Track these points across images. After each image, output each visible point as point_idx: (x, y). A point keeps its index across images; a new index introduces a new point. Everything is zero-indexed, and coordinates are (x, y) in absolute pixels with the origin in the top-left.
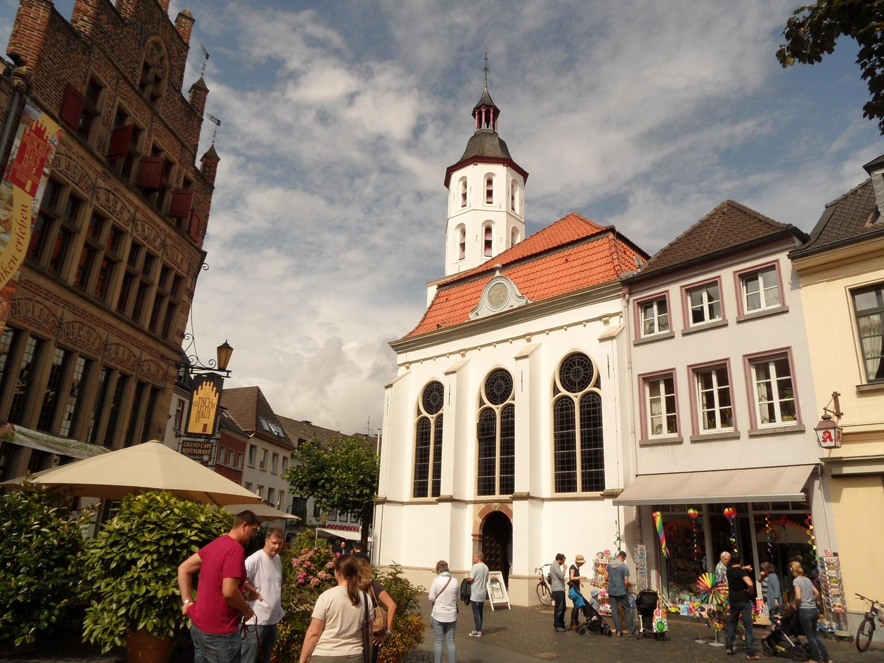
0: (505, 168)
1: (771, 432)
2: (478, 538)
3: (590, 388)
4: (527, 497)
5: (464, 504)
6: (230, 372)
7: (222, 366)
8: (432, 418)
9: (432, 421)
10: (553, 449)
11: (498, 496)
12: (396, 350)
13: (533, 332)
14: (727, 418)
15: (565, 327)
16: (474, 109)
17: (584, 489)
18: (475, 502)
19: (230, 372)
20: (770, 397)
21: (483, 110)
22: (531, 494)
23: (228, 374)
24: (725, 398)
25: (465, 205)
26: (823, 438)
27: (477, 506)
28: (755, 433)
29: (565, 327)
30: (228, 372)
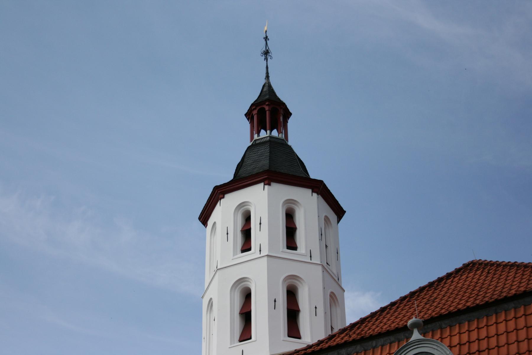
16: (252, 105)
21: (267, 108)
25: (250, 249)
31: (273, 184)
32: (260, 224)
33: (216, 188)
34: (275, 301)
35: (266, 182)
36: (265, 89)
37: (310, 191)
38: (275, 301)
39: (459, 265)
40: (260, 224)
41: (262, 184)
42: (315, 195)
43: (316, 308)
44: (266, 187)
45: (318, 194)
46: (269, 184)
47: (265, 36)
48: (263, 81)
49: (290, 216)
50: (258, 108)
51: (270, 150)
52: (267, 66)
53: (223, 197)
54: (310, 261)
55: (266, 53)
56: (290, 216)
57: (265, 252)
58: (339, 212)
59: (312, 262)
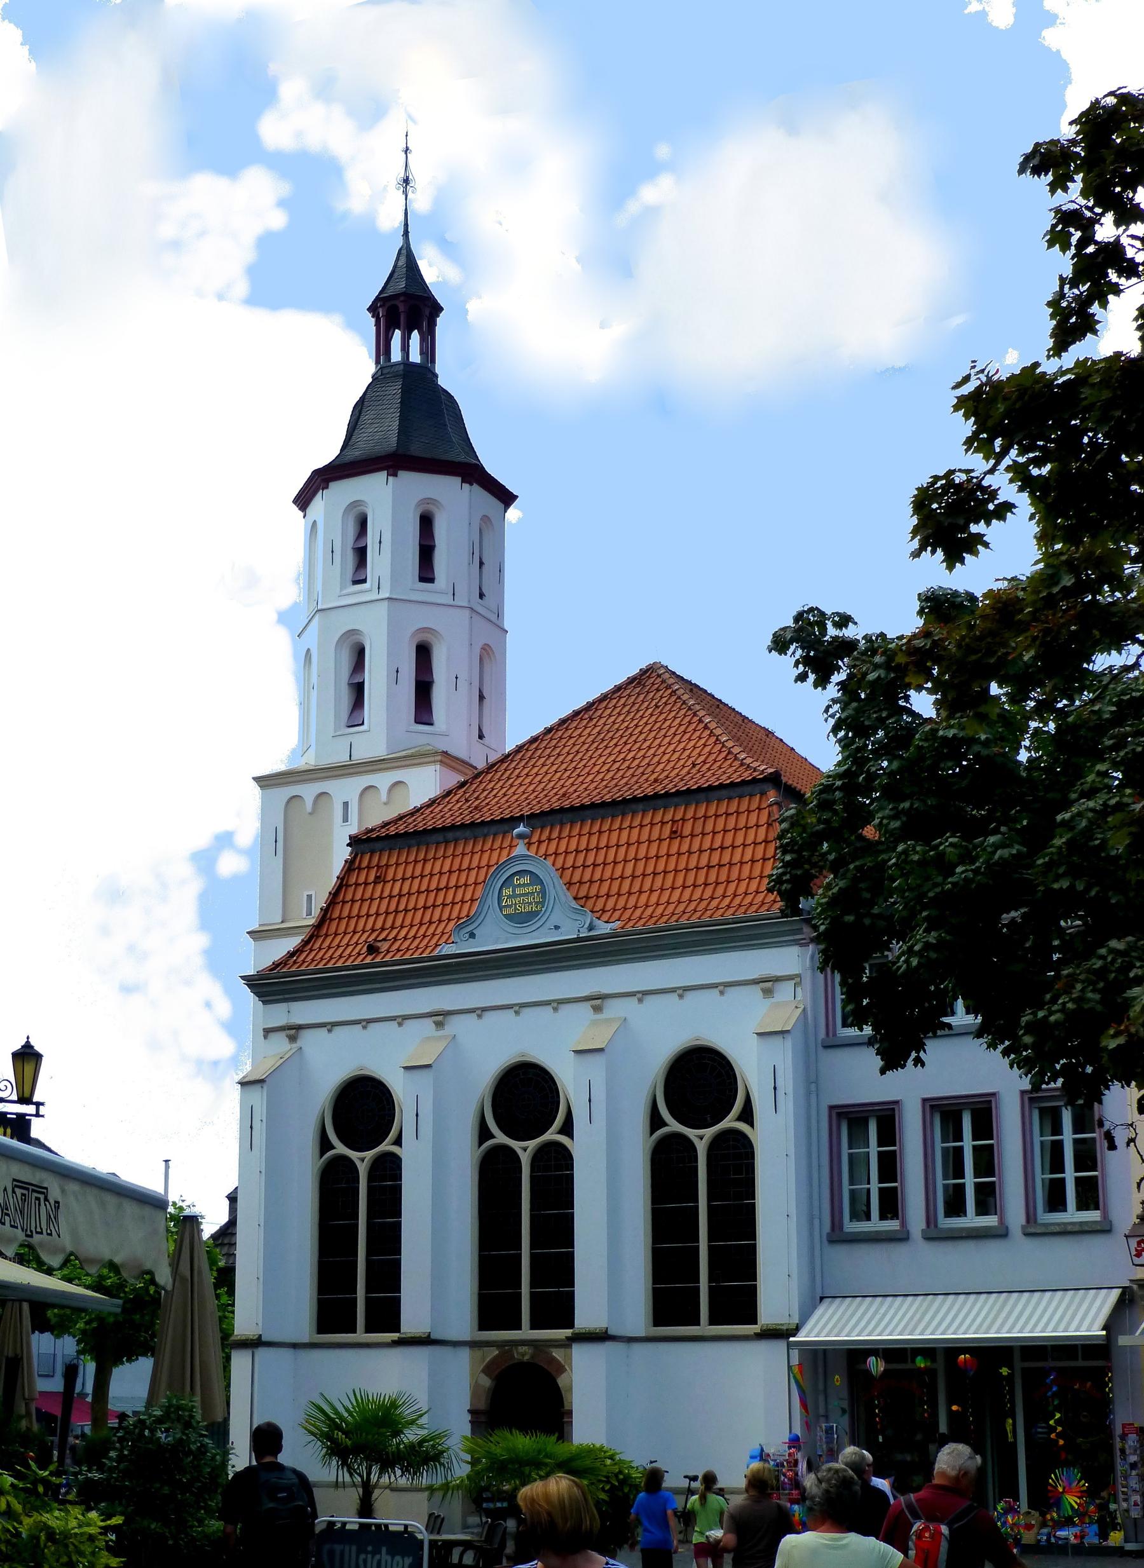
1: (1058, 1229)
2: (483, 1419)
3: (729, 1122)
6: (42, 1104)
7: (27, 1095)
8: (363, 1160)
11: (526, 1332)
12: (259, 995)
13: (606, 992)
14: (987, 1199)
15: (680, 992)
18: (473, 1345)
19: (42, 1104)
20: (1057, 1164)
21: (402, 308)
23: (38, 1110)
24: (986, 1161)
25: (364, 581)
26: (1136, 1250)
27: (478, 1353)
28: (1032, 1230)
29: (680, 992)
30: (38, 1104)
31: (401, 473)
32: (380, 542)
33: (317, 473)
34: (397, 671)
35: (391, 471)
36: (400, 263)
37: (459, 479)
38: (397, 671)
39: (634, 671)
40: (380, 542)
42: (466, 486)
43: (457, 678)
44: (391, 478)
45: (471, 484)
46: (395, 475)
48: (400, 242)
49: (426, 522)
50: (388, 304)
51: (401, 398)
52: (406, 209)
54: (451, 602)
55: (406, 181)
56: (426, 522)
57: (385, 594)
58: (506, 498)
59: (455, 603)
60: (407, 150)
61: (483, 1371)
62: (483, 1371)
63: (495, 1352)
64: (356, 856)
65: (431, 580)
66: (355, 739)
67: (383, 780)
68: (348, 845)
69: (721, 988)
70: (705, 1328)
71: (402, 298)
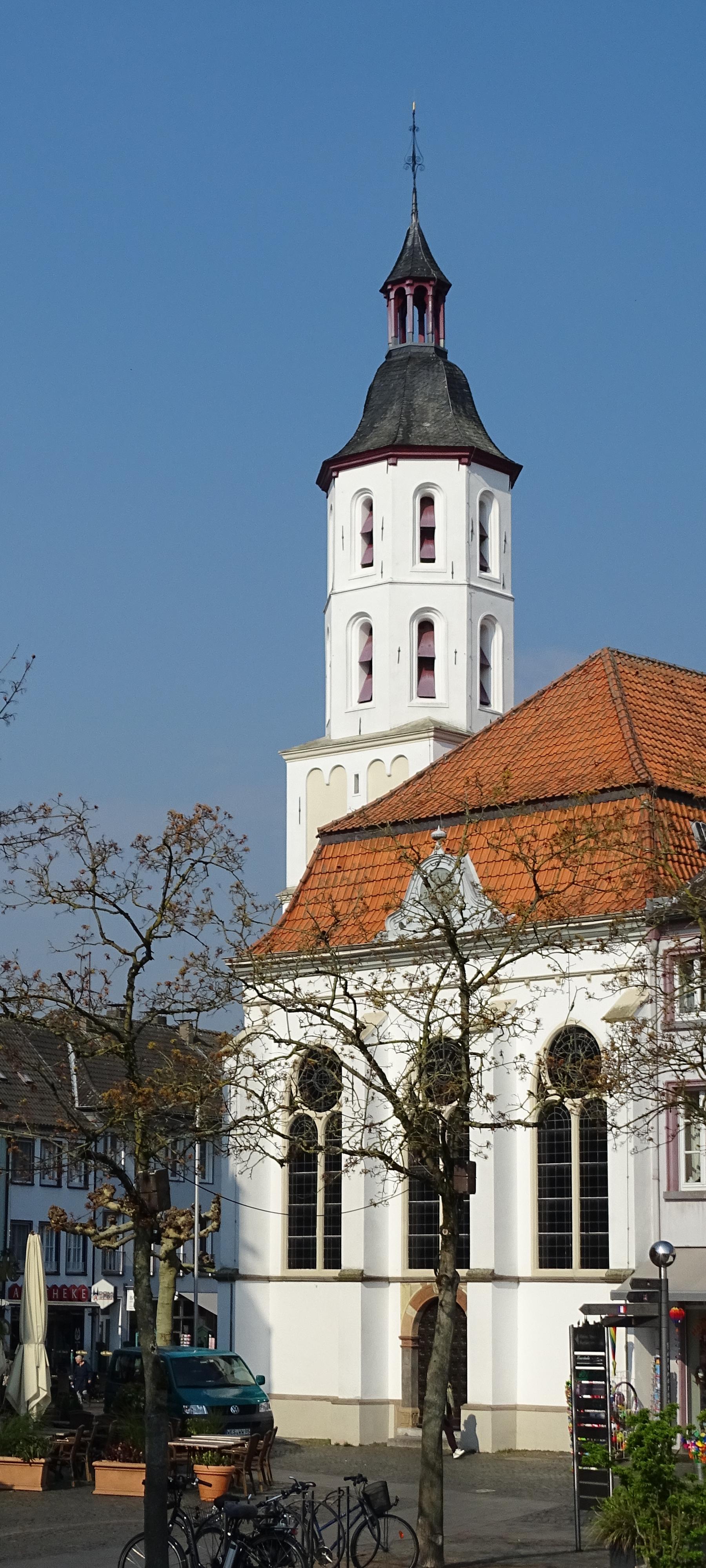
0: (464, 468)
2: (410, 1343)
4: (491, 1277)
5: (386, 1283)
9: (320, 1125)
10: (536, 1193)
17: (584, 1265)
18: (404, 1281)
21: (408, 290)
22: (496, 1272)
27: (407, 1286)
35: (391, 460)
37: (457, 462)
41: (385, 463)
44: (391, 467)
47: (412, 125)
53: (337, 476)
54: (450, 580)
59: (454, 581)
60: (414, 129)
61: (411, 1304)
62: (411, 1304)
63: (419, 1287)
64: (323, 846)
65: (432, 560)
66: (364, 716)
67: (387, 753)
68: (317, 837)
69: (588, 976)
70: (576, 1270)
71: (408, 282)
